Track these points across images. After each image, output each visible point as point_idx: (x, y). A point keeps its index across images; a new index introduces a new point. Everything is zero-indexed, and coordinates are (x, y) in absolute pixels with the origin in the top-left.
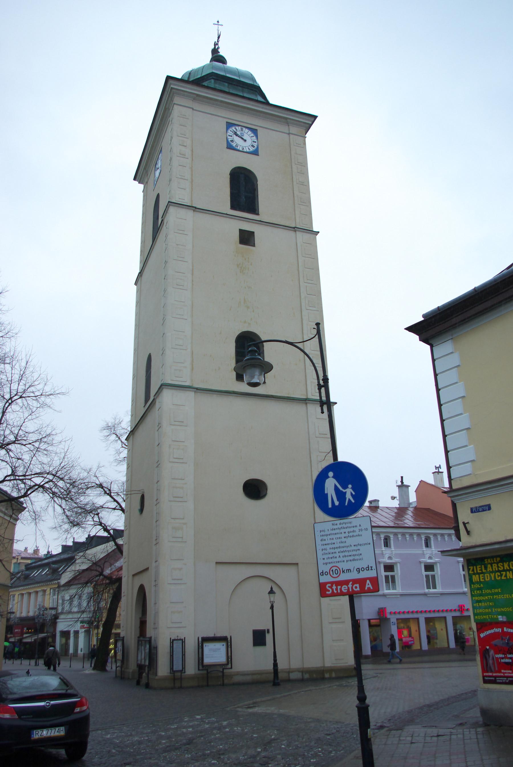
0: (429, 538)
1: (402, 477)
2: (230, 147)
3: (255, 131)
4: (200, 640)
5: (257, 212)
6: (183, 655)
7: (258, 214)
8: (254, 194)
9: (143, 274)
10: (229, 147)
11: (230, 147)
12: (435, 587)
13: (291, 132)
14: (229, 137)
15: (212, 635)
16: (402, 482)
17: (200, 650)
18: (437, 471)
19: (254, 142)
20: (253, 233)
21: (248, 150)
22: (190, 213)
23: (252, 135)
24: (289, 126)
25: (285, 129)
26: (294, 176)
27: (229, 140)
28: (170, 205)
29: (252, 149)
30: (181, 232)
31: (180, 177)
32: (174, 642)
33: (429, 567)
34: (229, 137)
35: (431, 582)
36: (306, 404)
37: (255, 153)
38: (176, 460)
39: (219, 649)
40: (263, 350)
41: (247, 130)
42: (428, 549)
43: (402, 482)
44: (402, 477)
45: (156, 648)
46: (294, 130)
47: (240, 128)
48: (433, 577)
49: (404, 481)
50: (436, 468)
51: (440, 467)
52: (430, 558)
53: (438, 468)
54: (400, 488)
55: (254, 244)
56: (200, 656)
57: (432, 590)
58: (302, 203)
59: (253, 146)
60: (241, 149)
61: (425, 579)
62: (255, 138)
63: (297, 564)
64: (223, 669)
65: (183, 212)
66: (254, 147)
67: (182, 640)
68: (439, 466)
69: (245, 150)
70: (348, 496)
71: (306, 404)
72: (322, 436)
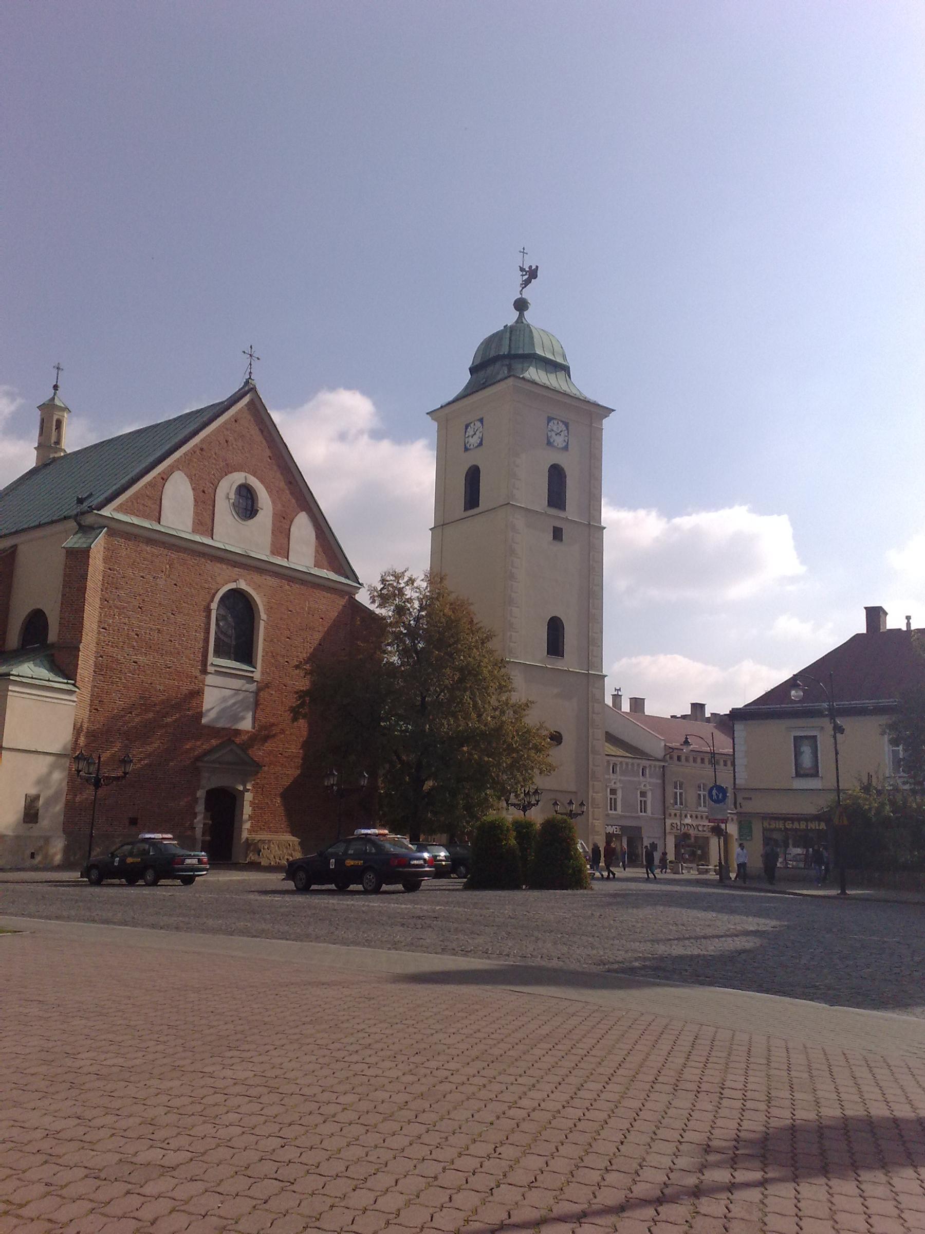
2: (549, 443)
3: (566, 425)
18: (616, 693)
20: (562, 529)
29: (564, 444)
48: (615, 799)
50: (616, 690)
51: (620, 690)
53: (618, 690)
70: (720, 797)
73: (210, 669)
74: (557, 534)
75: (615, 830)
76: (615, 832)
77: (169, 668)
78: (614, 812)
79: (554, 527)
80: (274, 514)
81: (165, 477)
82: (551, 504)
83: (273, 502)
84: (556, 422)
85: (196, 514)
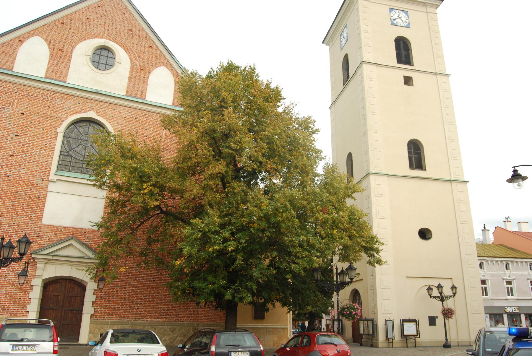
0: (508, 263)
1: (484, 224)
3: (406, 12)
4: (402, 321)
5: (412, 64)
6: (393, 329)
7: (413, 65)
8: (409, 52)
9: (336, 103)
10: (392, 24)
11: (393, 24)
12: (512, 295)
13: (428, 11)
14: (392, 18)
15: (408, 319)
16: (485, 227)
17: (402, 327)
18: (507, 220)
19: (406, 19)
20: (411, 78)
21: (404, 25)
22: (374, 67)
23: (405, 15)
24: (426, 7)
25: (423, 9)
26: (432, 40)
27: (392, 19)
28: (363, 63)
29: (406, 24)
30: (371, 79)
31: (366, 45)
32: (388, 322)
33: (509, 282)
34: (392, 18)
35: (510, 292)
36: (451, 182)
37: (408, 27)
38: (380, 217)
39: (412, 326)
40: (424, 150)
41: (402, 12)
42: (508, 271)
43: (485, 227)
44: (484, 224)
45: (376, 325)
46: (430, 9)
47: (397, 11)
48: (511, 289)
49: (486, 227)
50: (506, 218)
51: (509, 218)
52: (509, 276)
53: (508, 218)
54: (484, 231)
55: (413, 84)
56: (402, 330)
57: (511, 297)
58: (439, 57)
59: (407, 22)
60: (399, 25)
61: (506, 290)
62: (407, 17)
63: (452, 278)
64: (415, 338)
65: (370, 67)
66: (407, 22)
67: (392, 321)
68: (508, 217)
69: (402, 25)
71: (451, 182)
72: (461, 202)
73: (52, 177)
74: (408, 81)
75: (514, 310)
76: (514, 312)
77: (9, 176)
78: (512, 297)
79: (404, 76)
80: (132, 67)
81: (23, 39)
82: (399, 61)
83: (132, 60)
84: (397, 11)
85: (50, 64)
